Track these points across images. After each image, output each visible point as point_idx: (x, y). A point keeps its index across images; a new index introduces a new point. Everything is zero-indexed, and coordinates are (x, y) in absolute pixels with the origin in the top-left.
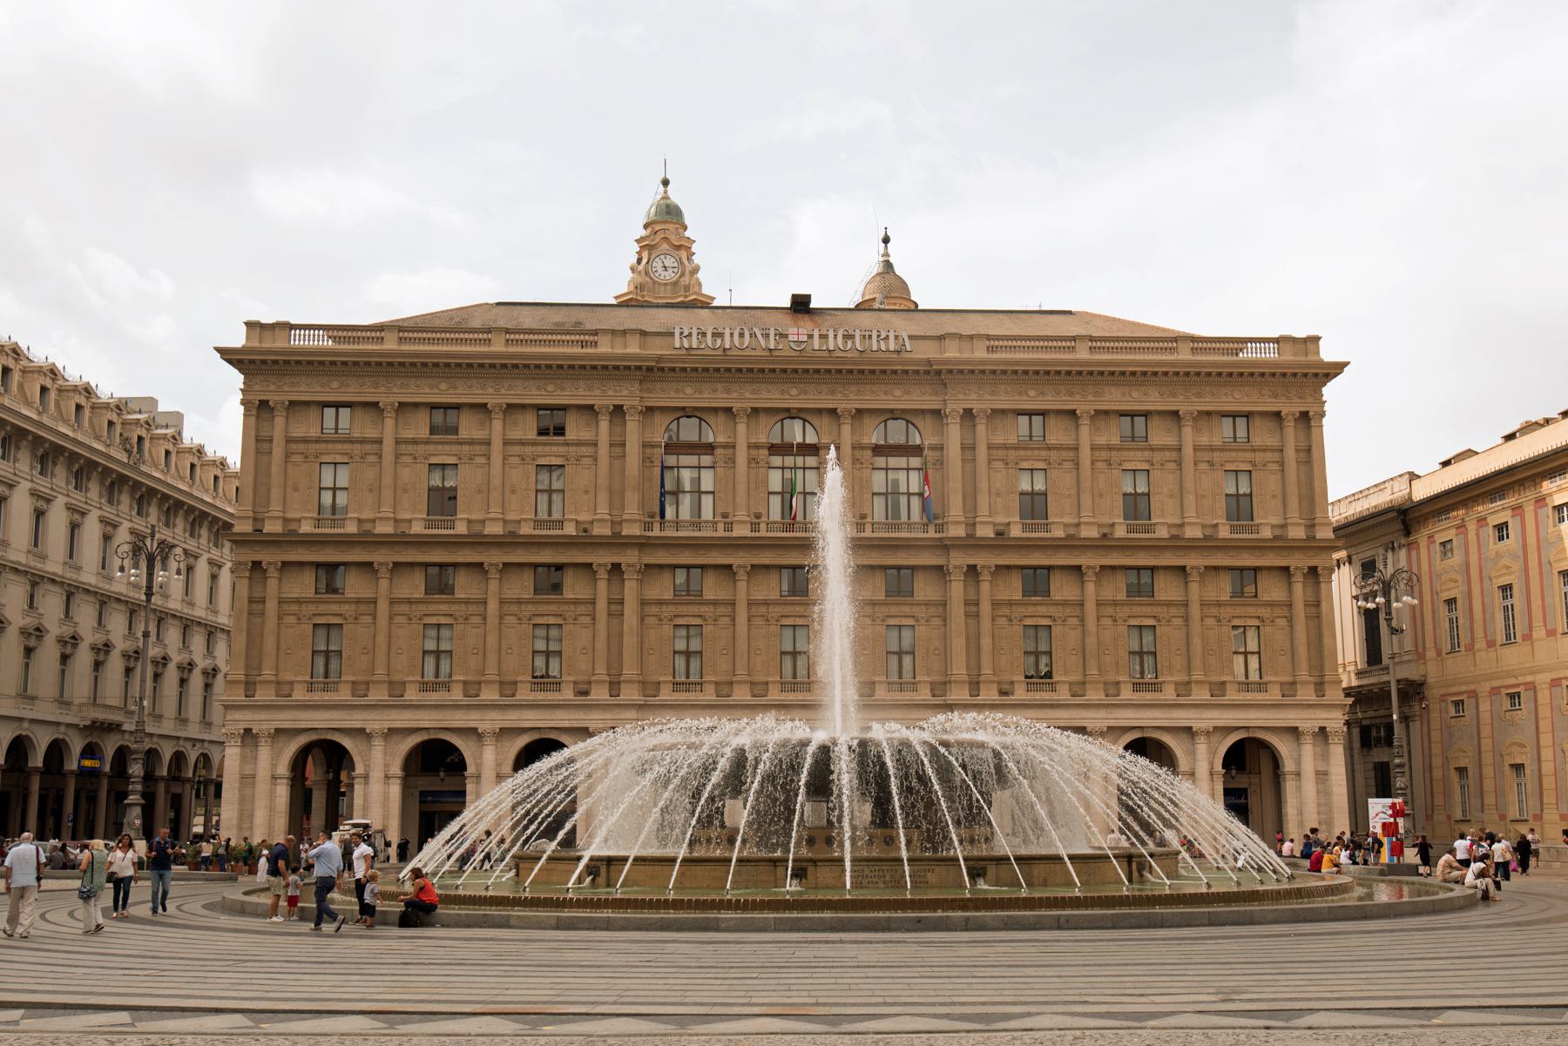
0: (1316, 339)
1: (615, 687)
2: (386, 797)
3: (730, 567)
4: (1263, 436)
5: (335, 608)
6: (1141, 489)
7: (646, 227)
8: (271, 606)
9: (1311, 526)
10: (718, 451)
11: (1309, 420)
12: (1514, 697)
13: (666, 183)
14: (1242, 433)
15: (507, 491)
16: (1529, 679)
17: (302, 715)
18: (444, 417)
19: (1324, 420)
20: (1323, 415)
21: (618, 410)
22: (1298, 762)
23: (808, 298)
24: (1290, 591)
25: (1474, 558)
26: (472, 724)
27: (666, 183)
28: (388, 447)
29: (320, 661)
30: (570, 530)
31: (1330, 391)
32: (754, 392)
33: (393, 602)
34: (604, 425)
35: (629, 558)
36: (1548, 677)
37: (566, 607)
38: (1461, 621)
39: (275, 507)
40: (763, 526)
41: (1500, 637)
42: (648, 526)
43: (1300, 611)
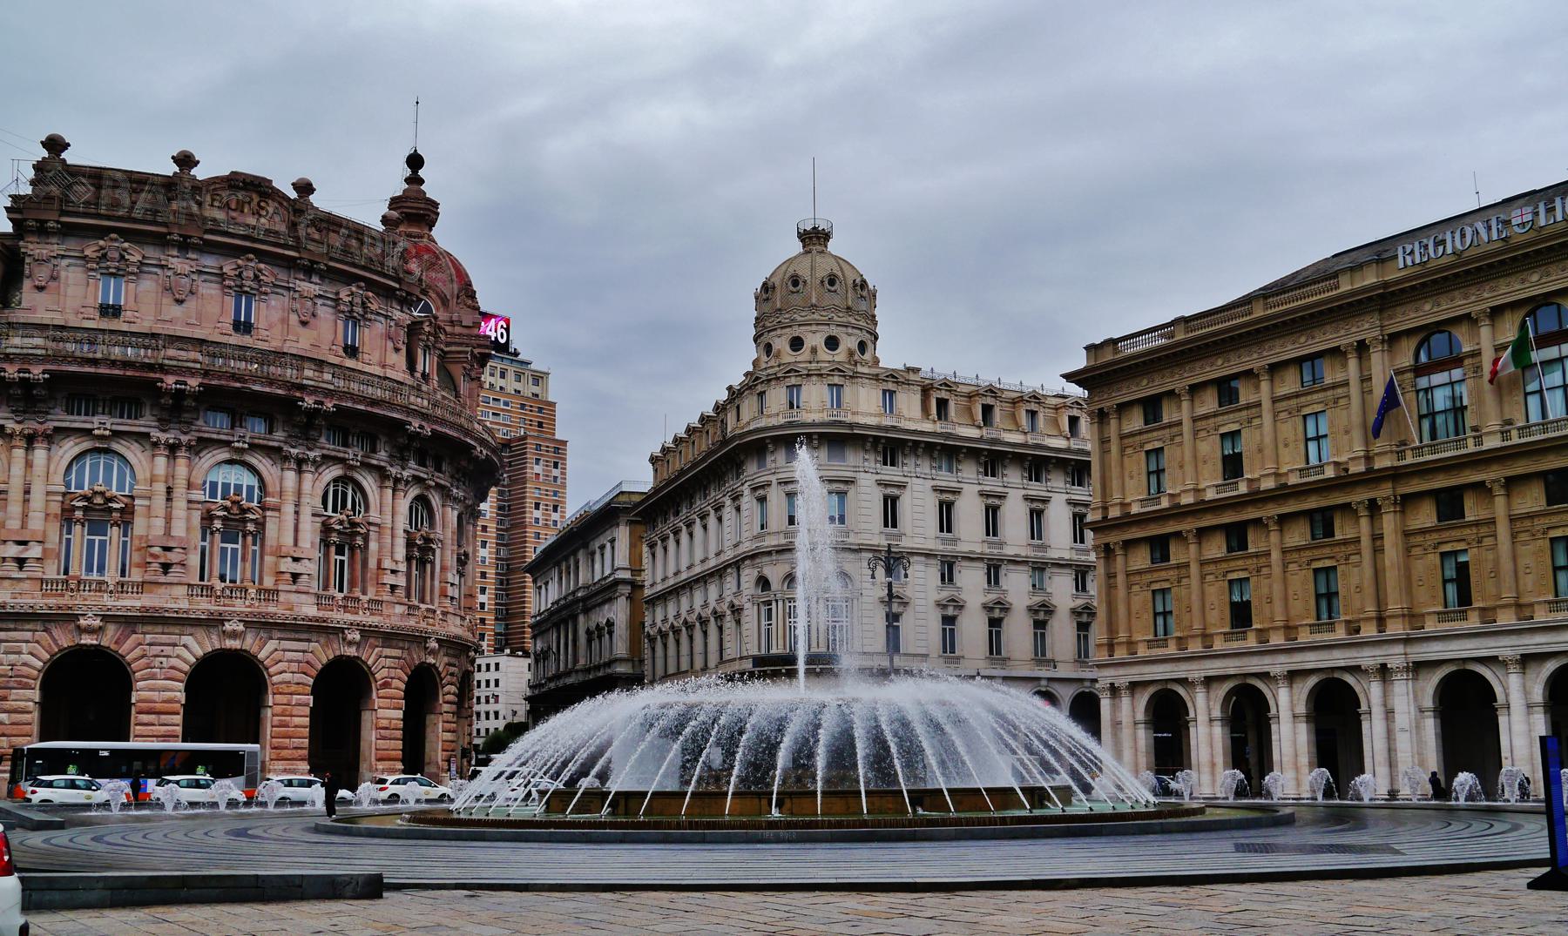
1: (1381, 621)
2: (1211, 735)
3: (1482, 483)
5: (1163, 575)
8: (1120, 579)
10: (1466, 362)
15: (1281, 446)
17: (1147, 669)
18: (1226, 389)
21: (1362, 348)
26: (1266, 669)
28: (1187, 427)
29: (1160, 621)
30: (1330, 473)
32: (1492, 290)
33: (1203, 563)
34: (1353, 363)
35: (1384, 491)
37: (1337, 549)
39: (1116, 497)
40: (1514, 433)
42: (1401, 455)
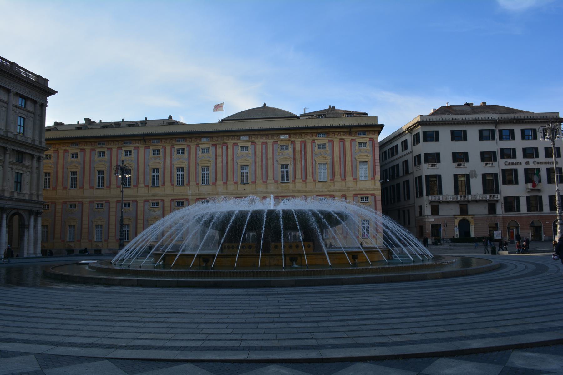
0: (48, 81)
4: (30, 107)
9: (40, 142)
11: (44, 106)
12: (73, 206)
14: (23, 104)
16: (80, 200)
19: (47, 108)
20: (47, 106)
22: (29, 221)
24: (32, 164)
25: (61, 161)
31: (50, 99)
36: (89, 200)
38: (51, 180)
41: (69, 186)
43: (35, 171)
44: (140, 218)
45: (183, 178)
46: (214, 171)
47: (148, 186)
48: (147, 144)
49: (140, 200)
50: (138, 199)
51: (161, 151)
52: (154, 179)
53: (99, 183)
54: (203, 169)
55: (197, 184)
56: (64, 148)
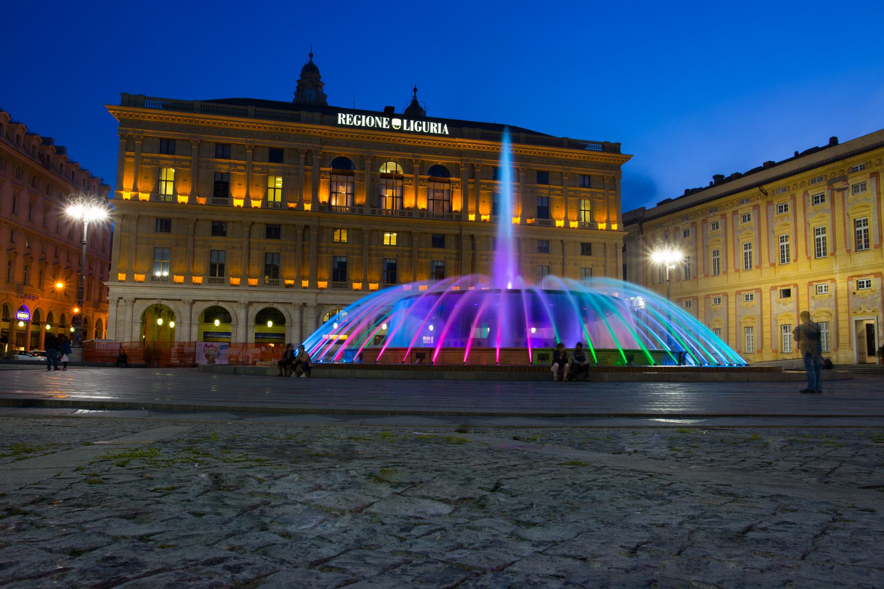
0: (620, 144)
6: (545, 205)
7: (301, 76)
13: (311, 55)
16: (695, 295)
23: (392, 109)
27: (311, 55)
36: (704, 294)
44: (766, 315)
45: (824, 244)
46: (876, 222)
47: (773, 265)
48: (769, 199)
49: (765, 288)
50: (762, 287)
51: (789, 204)
52: (783, 252)
53: (715, 268)
54: (857, 224)
55: (849, 251)
56: (674, 226)
